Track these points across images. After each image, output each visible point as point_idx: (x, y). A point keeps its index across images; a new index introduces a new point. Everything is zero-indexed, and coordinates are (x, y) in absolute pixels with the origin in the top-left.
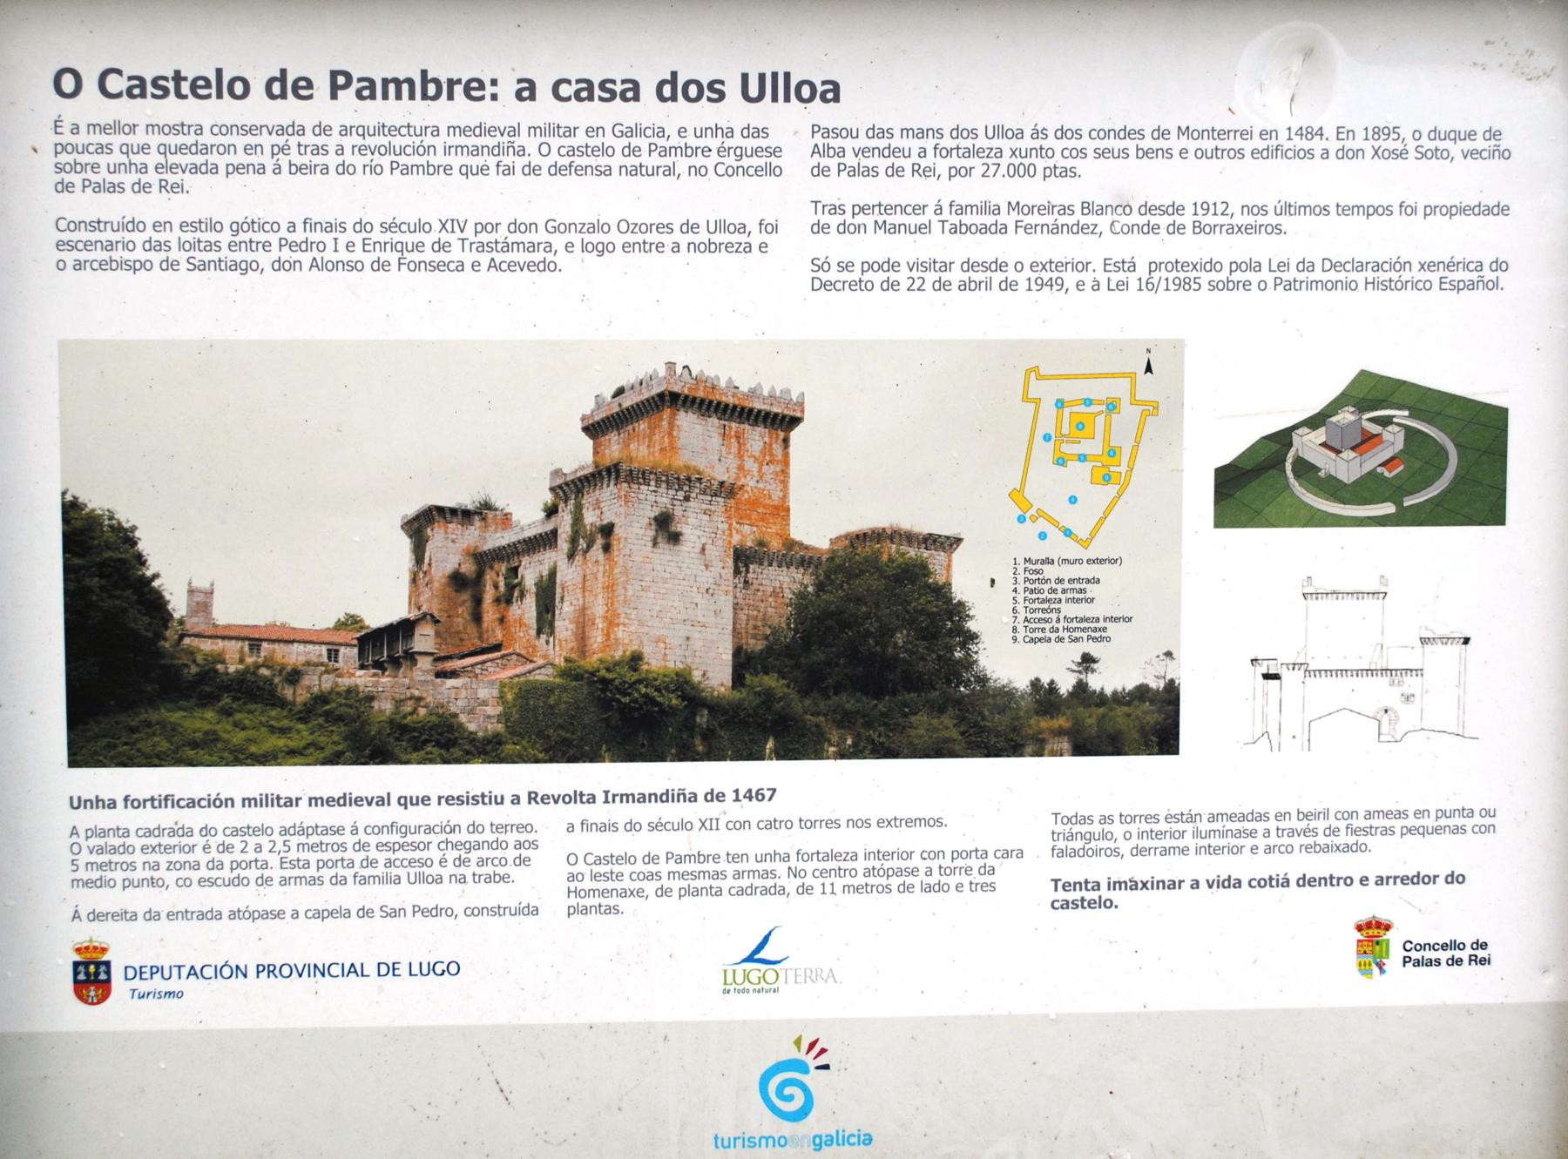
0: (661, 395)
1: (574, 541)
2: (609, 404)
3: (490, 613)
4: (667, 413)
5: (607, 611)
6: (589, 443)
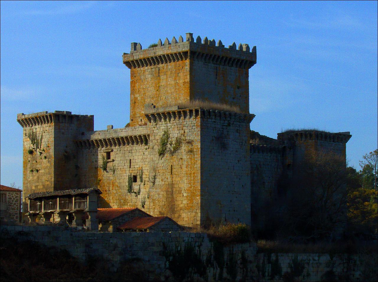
5: (191, 187)
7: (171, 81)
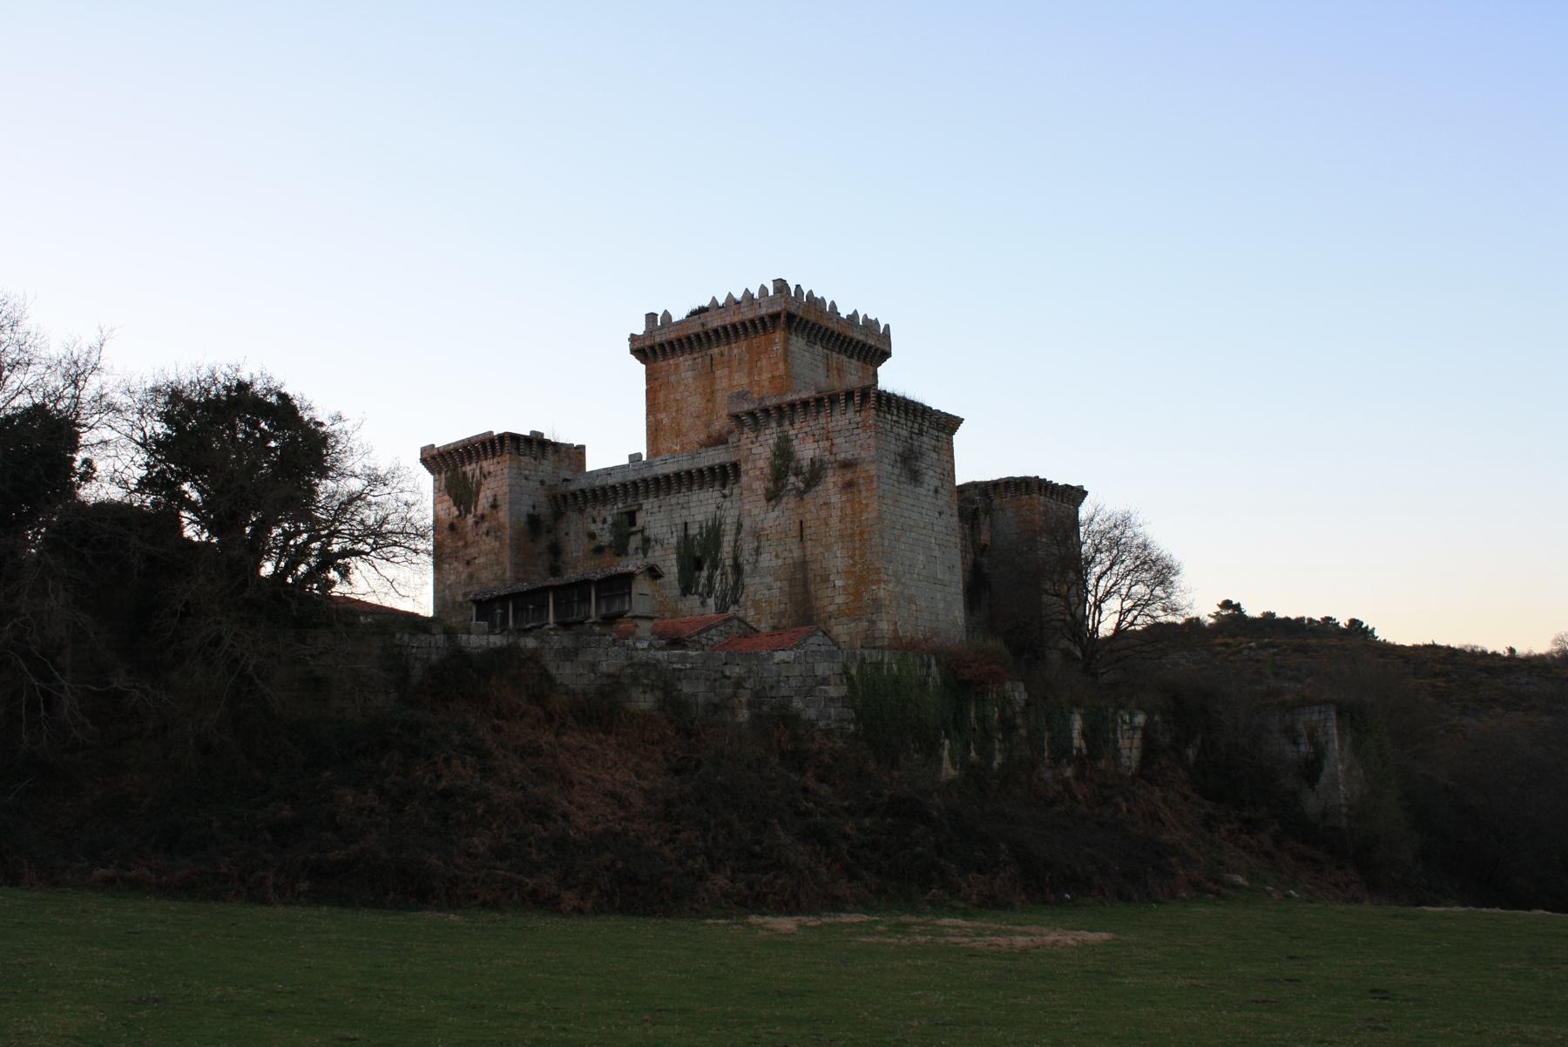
0: (775, 317)
4: (778, 337)
5: (854, 565)
6: (640, 369)
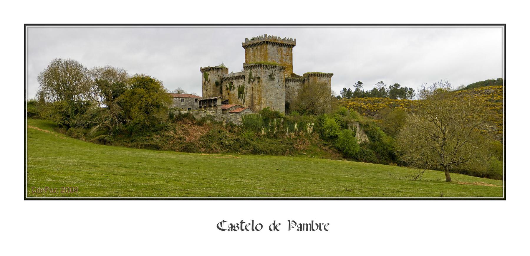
0: (264, 42)
1: (250, 79)
2: (250, 41)
3: (225, 93)
4: (265, 46)
7: (259, 53)
